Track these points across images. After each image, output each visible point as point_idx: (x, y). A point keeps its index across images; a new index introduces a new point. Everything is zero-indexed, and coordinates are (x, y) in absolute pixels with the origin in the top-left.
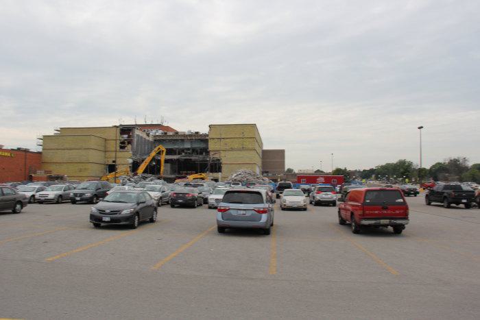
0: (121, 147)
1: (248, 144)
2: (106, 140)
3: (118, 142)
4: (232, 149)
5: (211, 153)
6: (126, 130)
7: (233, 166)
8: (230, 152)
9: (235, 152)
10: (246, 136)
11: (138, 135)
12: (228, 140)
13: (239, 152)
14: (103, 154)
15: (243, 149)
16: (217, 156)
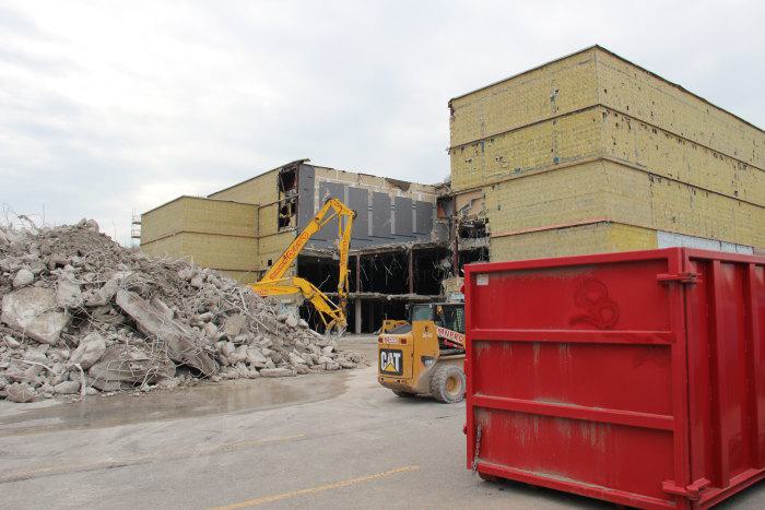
0: (283, 223)
1: (575, 139)
2: (260, 208)
3: (276, 206)
4: (520, 176)
5: (461, 203)
6: (289, 177)
7: (528, 240)
8: (514, 188)
9: (527, 184)
10: (563, 111)
11: (324, 185)
12: (507, 141)
13: (541, 181)
14: (250, 245)
15: (557, 166)
16: (475, 212)
